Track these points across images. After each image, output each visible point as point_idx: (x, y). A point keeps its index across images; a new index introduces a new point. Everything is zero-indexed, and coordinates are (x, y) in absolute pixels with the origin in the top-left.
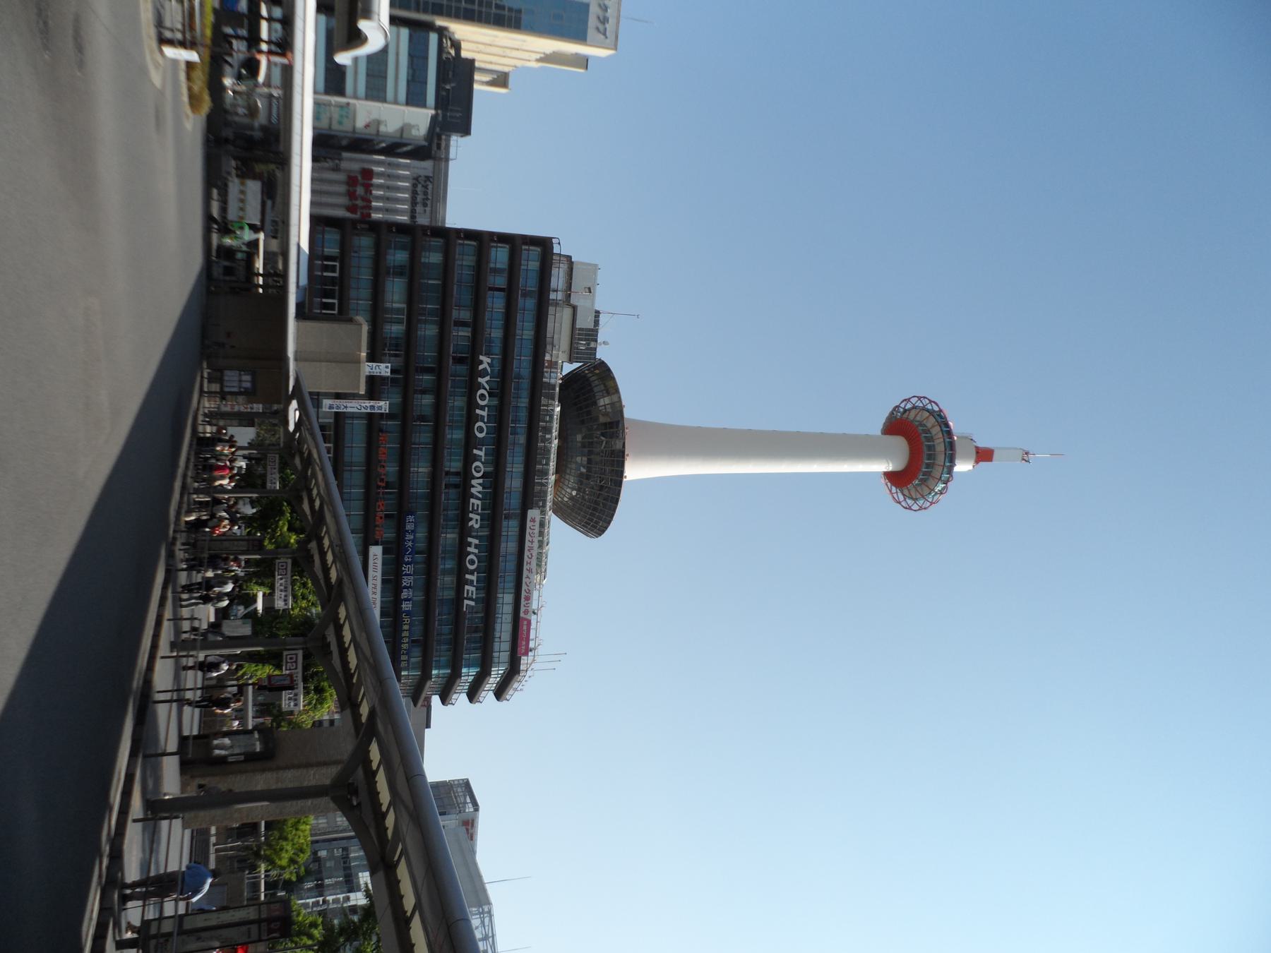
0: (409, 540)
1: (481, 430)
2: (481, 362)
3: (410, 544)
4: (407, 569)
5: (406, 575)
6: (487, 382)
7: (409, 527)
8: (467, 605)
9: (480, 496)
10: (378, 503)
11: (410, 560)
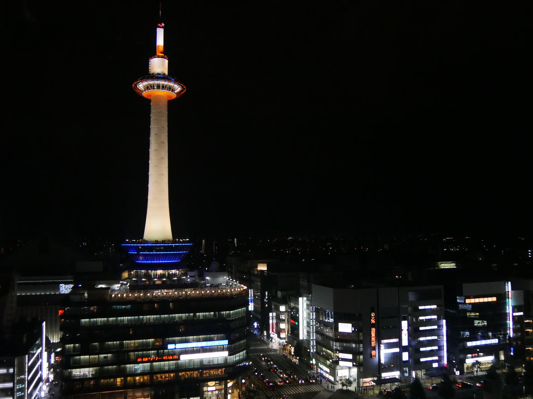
10: (164, 359)
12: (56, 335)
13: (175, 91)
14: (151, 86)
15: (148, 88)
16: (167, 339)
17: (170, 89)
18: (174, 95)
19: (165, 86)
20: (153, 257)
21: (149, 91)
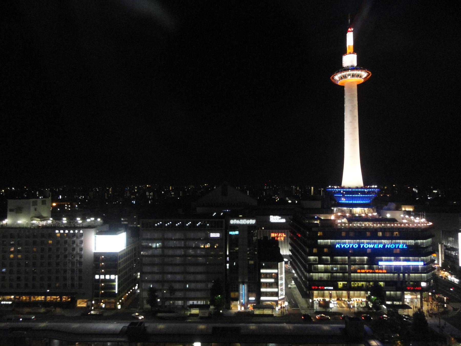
1: (356, 246)
2: (338, 247)
6: (343, 244)
8: (405, 246)
9: (374, 245)
12: (285, 250)
13: (362, 77)
14: (344, 77)
15: (341, 78)
16: (335, 257)
17: (358, 76)
18: (361, 80)
19: (354, 75)
20: (353, 198)
21: (342, 80)
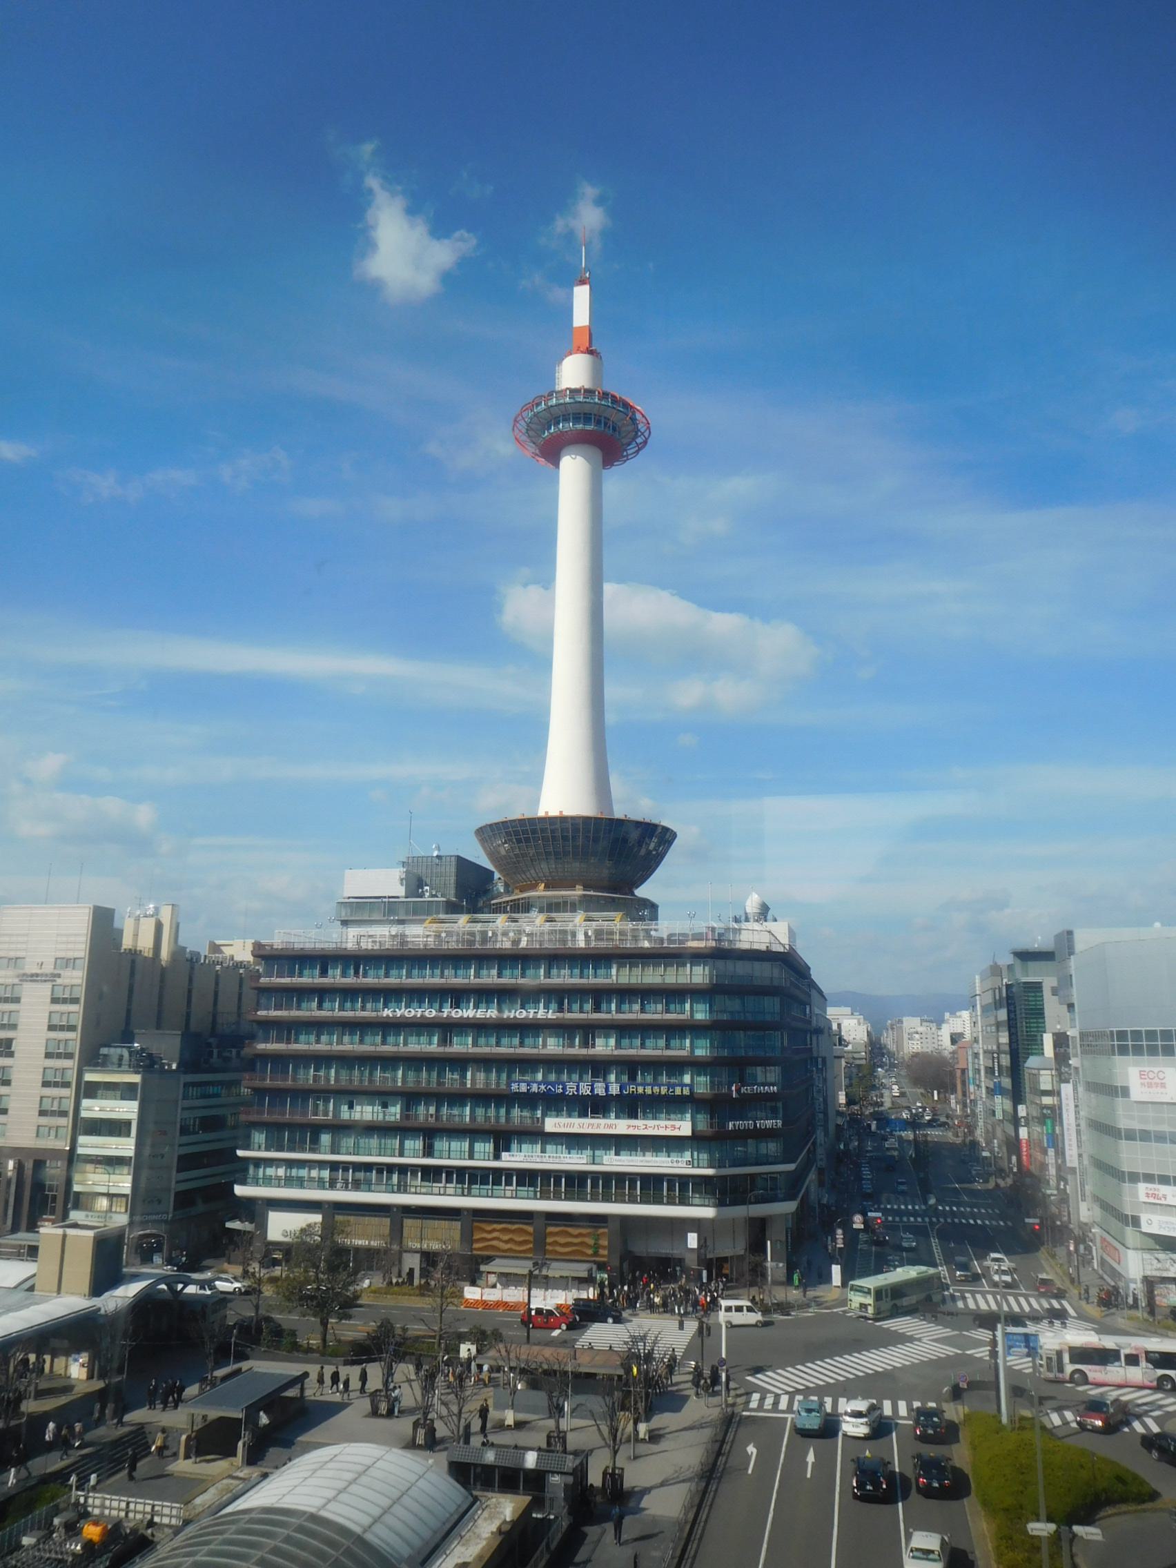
0: (539, 1088)
3: (543, 1087)
4: (571, 1089)
5: (578, 1090)
7: (523, 1088)
11: (561, 1087)
